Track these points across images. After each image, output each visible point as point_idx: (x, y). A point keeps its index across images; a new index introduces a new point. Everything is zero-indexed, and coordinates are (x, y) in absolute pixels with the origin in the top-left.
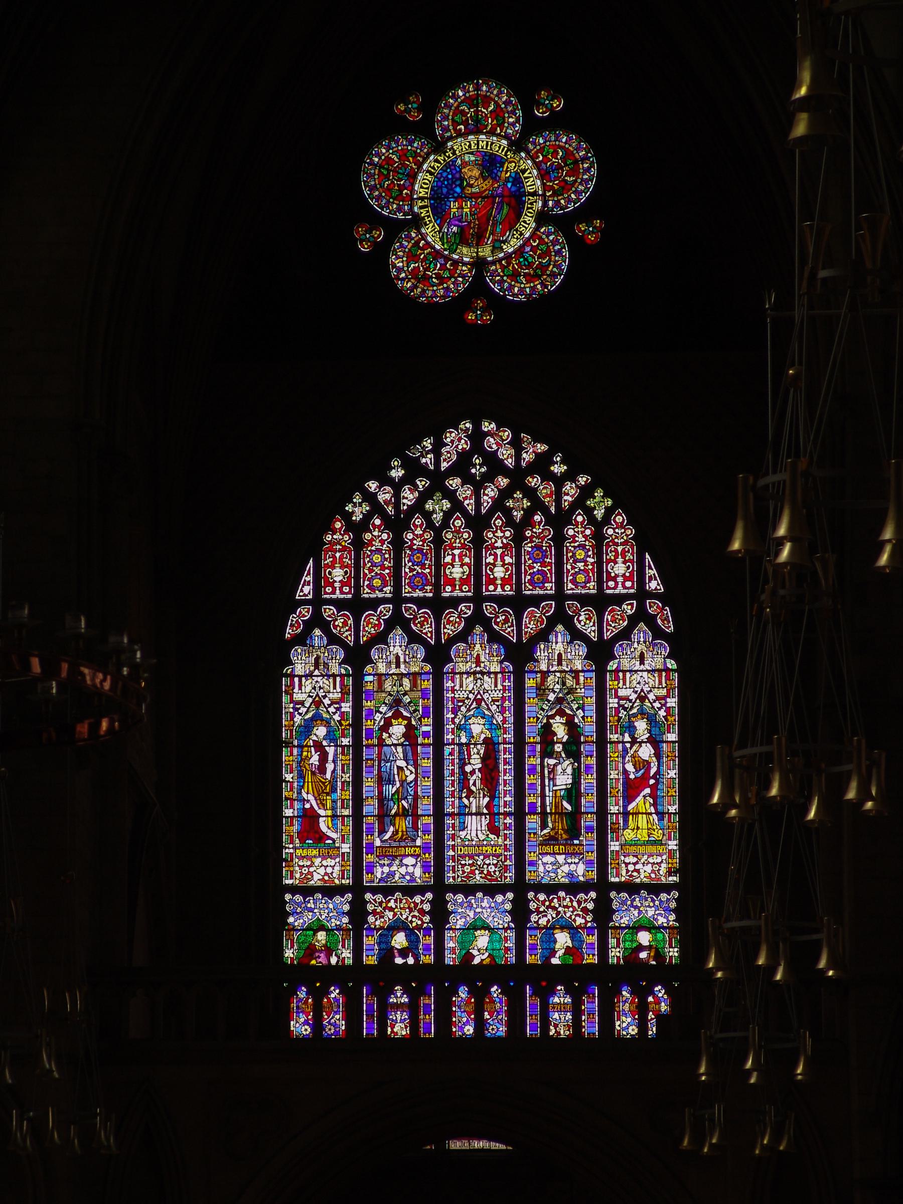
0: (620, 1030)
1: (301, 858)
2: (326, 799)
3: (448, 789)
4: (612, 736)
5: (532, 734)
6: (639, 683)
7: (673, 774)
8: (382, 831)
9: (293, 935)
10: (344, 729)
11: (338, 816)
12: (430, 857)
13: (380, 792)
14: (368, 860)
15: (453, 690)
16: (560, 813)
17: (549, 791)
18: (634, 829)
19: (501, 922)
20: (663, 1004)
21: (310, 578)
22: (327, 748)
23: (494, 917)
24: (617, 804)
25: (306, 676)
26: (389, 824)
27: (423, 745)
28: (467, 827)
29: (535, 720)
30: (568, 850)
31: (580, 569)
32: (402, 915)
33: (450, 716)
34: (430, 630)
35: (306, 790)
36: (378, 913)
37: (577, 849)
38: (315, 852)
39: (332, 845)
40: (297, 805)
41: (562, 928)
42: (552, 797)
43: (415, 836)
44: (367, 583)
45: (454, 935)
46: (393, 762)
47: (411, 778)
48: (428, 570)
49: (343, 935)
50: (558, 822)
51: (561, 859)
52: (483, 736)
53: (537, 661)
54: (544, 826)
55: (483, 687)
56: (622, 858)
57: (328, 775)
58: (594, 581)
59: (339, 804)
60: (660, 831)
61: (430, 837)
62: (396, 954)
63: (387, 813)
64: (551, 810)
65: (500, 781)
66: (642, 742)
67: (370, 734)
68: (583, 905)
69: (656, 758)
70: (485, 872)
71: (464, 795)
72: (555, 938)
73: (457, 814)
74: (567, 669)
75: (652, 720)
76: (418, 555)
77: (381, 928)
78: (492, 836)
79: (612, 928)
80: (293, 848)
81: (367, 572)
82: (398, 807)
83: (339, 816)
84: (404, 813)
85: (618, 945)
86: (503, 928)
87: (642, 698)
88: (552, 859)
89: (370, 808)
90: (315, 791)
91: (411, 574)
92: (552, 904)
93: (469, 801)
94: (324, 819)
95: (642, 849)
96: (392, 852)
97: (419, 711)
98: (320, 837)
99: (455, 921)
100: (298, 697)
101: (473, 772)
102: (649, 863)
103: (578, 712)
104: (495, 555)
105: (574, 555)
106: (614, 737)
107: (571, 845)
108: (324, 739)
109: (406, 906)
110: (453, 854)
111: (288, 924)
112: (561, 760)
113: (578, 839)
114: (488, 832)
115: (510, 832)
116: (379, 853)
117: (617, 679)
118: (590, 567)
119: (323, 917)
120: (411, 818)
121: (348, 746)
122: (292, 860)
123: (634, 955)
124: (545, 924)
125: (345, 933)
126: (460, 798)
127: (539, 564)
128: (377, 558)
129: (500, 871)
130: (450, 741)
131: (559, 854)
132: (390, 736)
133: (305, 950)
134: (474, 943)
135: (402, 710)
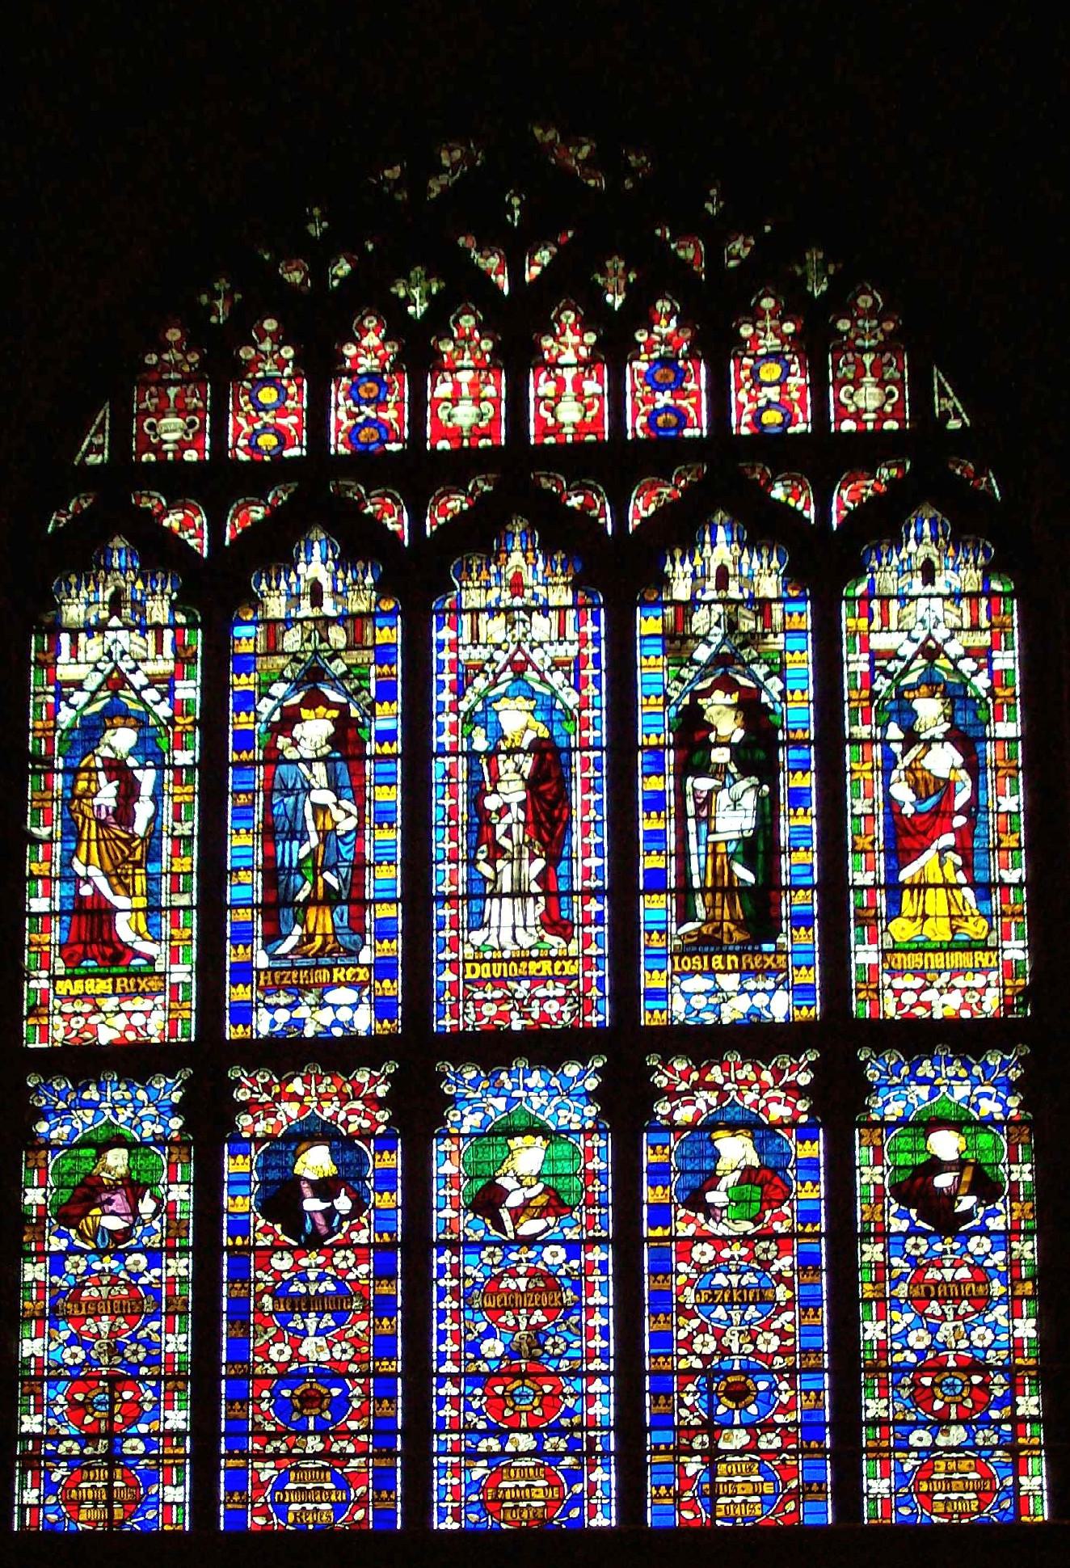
1: (70, 998)
2: (134, 875)
3: (442, 843)
4: (855, 729)
6: (922, 621)
7: (1011, 803)
8: (273, 936)
9: (46, 1159)
10: (182, 733)
11: (160, 909)
12: (392, 988)
13: (270, 859)
14: (235, 998)
16: (728, 889)
17: (698, 844)
19: (576, 1118)
20: (996, 1283)
21: (103, 440)
22: (138, 774)
25: (90, 630)
26: (291, 920)
27: (377, 758)
29: (661, 700)
30: (748, 965)
31: (769, 402)
33: (447, 697)
35: (83, 856)
38: (104, 986)
39: (148, 969)
41: (733, 1127)
42: (707, 854)
43: (355, 943)
44: (242, 442)
49: (170, 1154)
50: (722, 907)
51: (730, 982)
52: (530, 736)
54: (685, 914)
56: (887, 979)
57: (140, 827)
59: (166, 882)
60: (984, 922)
62: (307, 1192)
63: (285, 897)
64: (703, 881)
66: (933, 740)
70: (536, 1015)
72: (718, 1151)
74: (739, 596)
75: (956, 695)
76: (369, 385)
77: (268, 1137)
80: (48, 978)
81: (242, 421)
82: (315, 885)
83: (166, 909)
84: (330, 899)
85: (878, 1160)
86: (582, 1130)
87: (931, 653)
88: (708, 984)
89: (245, 887)
91: (351, 423)
92: (708, 1078)
93: (495, 869)
95: (937, 960)
96: (298, 978)
97: (369, 691)
98: (116, 955)
99: (458, 1118)
100: (65, 672)
101: (505, 809)
102: (954, 987)
103: (769, 683)
104: (561, 382)
105: (755, 373)
106: (862, 731)
107: (754, 953)
109: (334, 1089)
110: (454, 978)
113: (773, 941)
114: (543, 932)
115: (600, 929)
119: (122, 1119)
120: (345, 908)
121: (190, 768)
122: (45, 1004)
125: (175, 1150)
126: (472, 862)
127: (668, 393)
128: (268, 395)
129: (573, 1013)
130: (447, 748)
131: (725, 972)
132: (295, 743)
133: (74, 1188)
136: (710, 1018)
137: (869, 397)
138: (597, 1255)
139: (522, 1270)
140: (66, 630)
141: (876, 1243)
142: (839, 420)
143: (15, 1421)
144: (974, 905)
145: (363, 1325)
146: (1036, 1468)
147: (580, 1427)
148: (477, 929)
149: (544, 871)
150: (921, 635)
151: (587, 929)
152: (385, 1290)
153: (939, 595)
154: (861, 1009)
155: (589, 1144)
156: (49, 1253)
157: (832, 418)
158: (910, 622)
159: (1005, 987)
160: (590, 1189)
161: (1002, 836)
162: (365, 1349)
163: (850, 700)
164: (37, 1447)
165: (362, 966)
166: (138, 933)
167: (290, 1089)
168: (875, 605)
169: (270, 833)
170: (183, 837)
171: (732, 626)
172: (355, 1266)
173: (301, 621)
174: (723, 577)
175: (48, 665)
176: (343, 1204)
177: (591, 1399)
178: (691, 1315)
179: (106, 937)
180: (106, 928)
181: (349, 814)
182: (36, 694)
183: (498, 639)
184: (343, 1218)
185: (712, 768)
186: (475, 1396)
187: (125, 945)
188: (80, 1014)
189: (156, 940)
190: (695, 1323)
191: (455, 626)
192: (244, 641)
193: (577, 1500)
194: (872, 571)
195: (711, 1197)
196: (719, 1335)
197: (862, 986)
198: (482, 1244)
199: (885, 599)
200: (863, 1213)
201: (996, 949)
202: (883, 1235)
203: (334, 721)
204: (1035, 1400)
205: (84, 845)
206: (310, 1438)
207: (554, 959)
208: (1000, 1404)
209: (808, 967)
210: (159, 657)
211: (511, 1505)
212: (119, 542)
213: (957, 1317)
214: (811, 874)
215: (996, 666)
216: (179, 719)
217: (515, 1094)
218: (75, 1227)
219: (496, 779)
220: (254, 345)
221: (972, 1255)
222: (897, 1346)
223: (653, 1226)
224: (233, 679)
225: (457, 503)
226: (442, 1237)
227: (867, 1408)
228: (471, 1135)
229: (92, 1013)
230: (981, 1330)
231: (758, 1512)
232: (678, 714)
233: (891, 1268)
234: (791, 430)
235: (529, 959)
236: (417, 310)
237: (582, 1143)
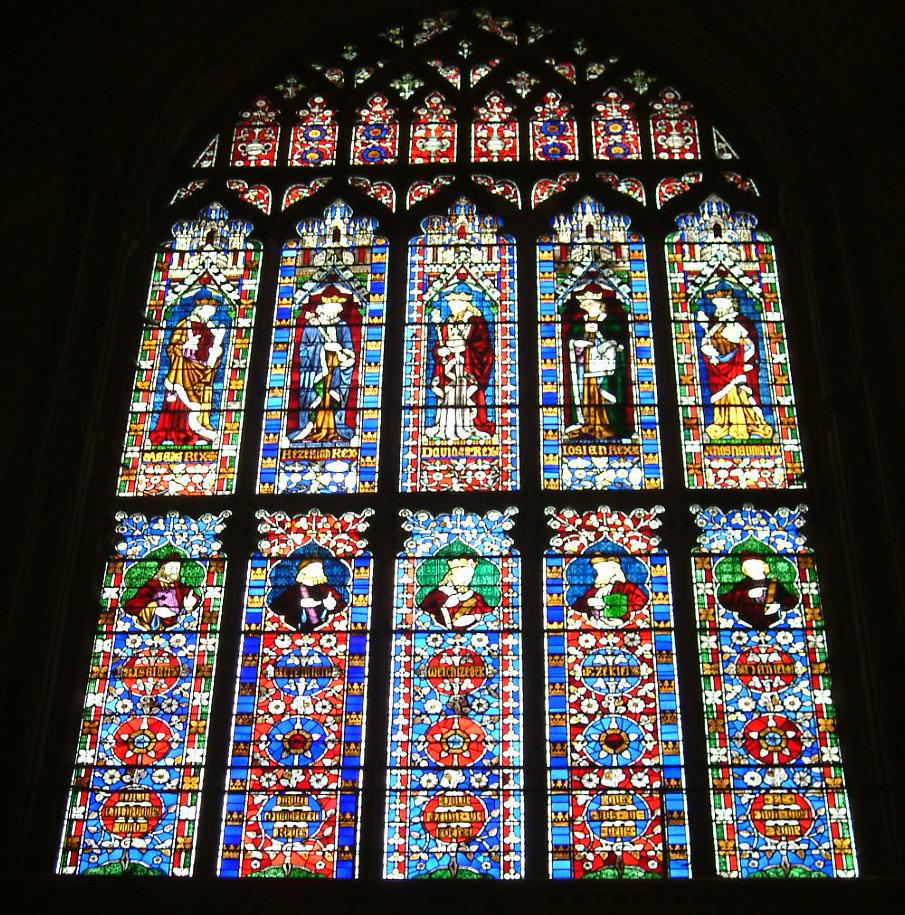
0: (722, 705)
2: (204, 390)
3: (408, 375)
4: (677, 315)
5: (547, 308)
8: (293, 428)
9: (122, 568)
11: (220, 411)
13: (295, 383)
15: (421, 264)
17: (578, 378)
18: (723, 425)
19: (496, 548)
20: (799, 665)
21: (214, 154)
22: (213, 331)
23: (483, 541)
24: (692, 393)
25: (192, 252)
26: (306, 419)
29: (553, 296)
30: (613, 452)
31: (615, 143)
33: (416, 292)
34: (389, 201)
35: (172, 379)
38: (177, 457)
41: (606, 556)
43: (349, 434)
44: (296, 157)
47: (347, 363)
48: (390, 144)
49: (210, 566)
50: (595, 416)
51: (601, 462)
52: (468, 315)
53: (555, 233)
54: (570, 420)
55: (469, 260)
56: (707, 462)
57: (211, 362)
59: (225, 395)
60: (769, 428)
62: (305, 593)
65: (496, 366)
66: (727, 321)
69: (751, 339)
70: (469, 481)
71: (435, 383)
72: (595, 570)
73: (422, 408)
74: (601, 241)
75: (740, 297)
78: (483, 434)
81: (297, 146)
83: (224, 411)
84: (334, 407)
85: (709, 579)
86: (501, 556)
89: (276, 400)
90: (188, 382)
91: (364, 148)
92: (588, 523)
95: (740, 451)
96: (309, 455)
97: (366, 287)
98: (185, 437)
99: (414, 546)
100: (174, 273)
102: (752, 468)
103: (621, 288)
105: (606, 129)
106: (682, 316)
107: (617, 445)
108: (210, 320)
109: (328, 526)
110: (414, 456)
111: (117, 553)
112: (597, 342)
114: (475, 429)
115: (513, 428)
116: (287, 456)
117: (683, 252)
118: (631, 140)
120: (344, 412)
122: (135, 467)
123: (738, 593)
126: (429, 387)
128: (314, 134)
131: (598, 456)
132: (317, 316)
133: (140, 588)
135: (339, 287)
136: (588, 485)
137: (675, 141)
139: (456, 650)
140: (178, 251)
142: (657, 153)
143: (74, 753)
144: (762, 418)
145: (339, 688)
146: (841, 801)
147: (497, 766)
148: (431, 427)
150: (717, 264)
151: (505, 428)
152: (357, 663)
153: (725, 243)
154: (691, 482)
155: (505, 565)
156: (116, 633)
157: (654, 151)
158: (708, 257)
159: (787, 469)
160: (506, 595)
162: (339, 706)
163: (673, 298)
164: (88, 774)
165: (352, 448)
166: (203, 425)
167: (298, 525)
169: (296, 367)
170: (239, 368)
171: (597, 257)
173: (325, 249)
174: (590, 230)
175: (164, 269)
176: (330, 602)
177: (506, 744)
178: (579, 684)
179: (182, 427)
180: (182, 421)
181: (349, 357)
184: (329, 612)
185: (586, 335)
186: (419, 742)
190: (582, 691)
191: (422, 253)
192: (289, 259)
193: (495, 821)
194: (683, 229)
195: (591, 602)
196: (600, 699)
197: (691, 466)
198: (429, 632)
200: (700, 615)
202: (715, 630)
203: (343, 304)
206: (294, 771)
207: (482, 447)
208: (811, 752)
209: (654, 454)
210: (234, 267)
211: (444, 825)
212: (217, 206)
215: (764, 281)
217: (454, 531)
218: (137, 615)
219: (446, 339)
220: (308, 109)
222: (731, 709)
223: (551, 622)
226: (399, 626)
227: (711, 755)
228: (423, 558)
230: (791, 699)
231: (634, 834)
232: (563, 304)
233: (723, 653)
234: (629, 157)
235: (465, 446)
236: (407, 95)
237: (500, 564)
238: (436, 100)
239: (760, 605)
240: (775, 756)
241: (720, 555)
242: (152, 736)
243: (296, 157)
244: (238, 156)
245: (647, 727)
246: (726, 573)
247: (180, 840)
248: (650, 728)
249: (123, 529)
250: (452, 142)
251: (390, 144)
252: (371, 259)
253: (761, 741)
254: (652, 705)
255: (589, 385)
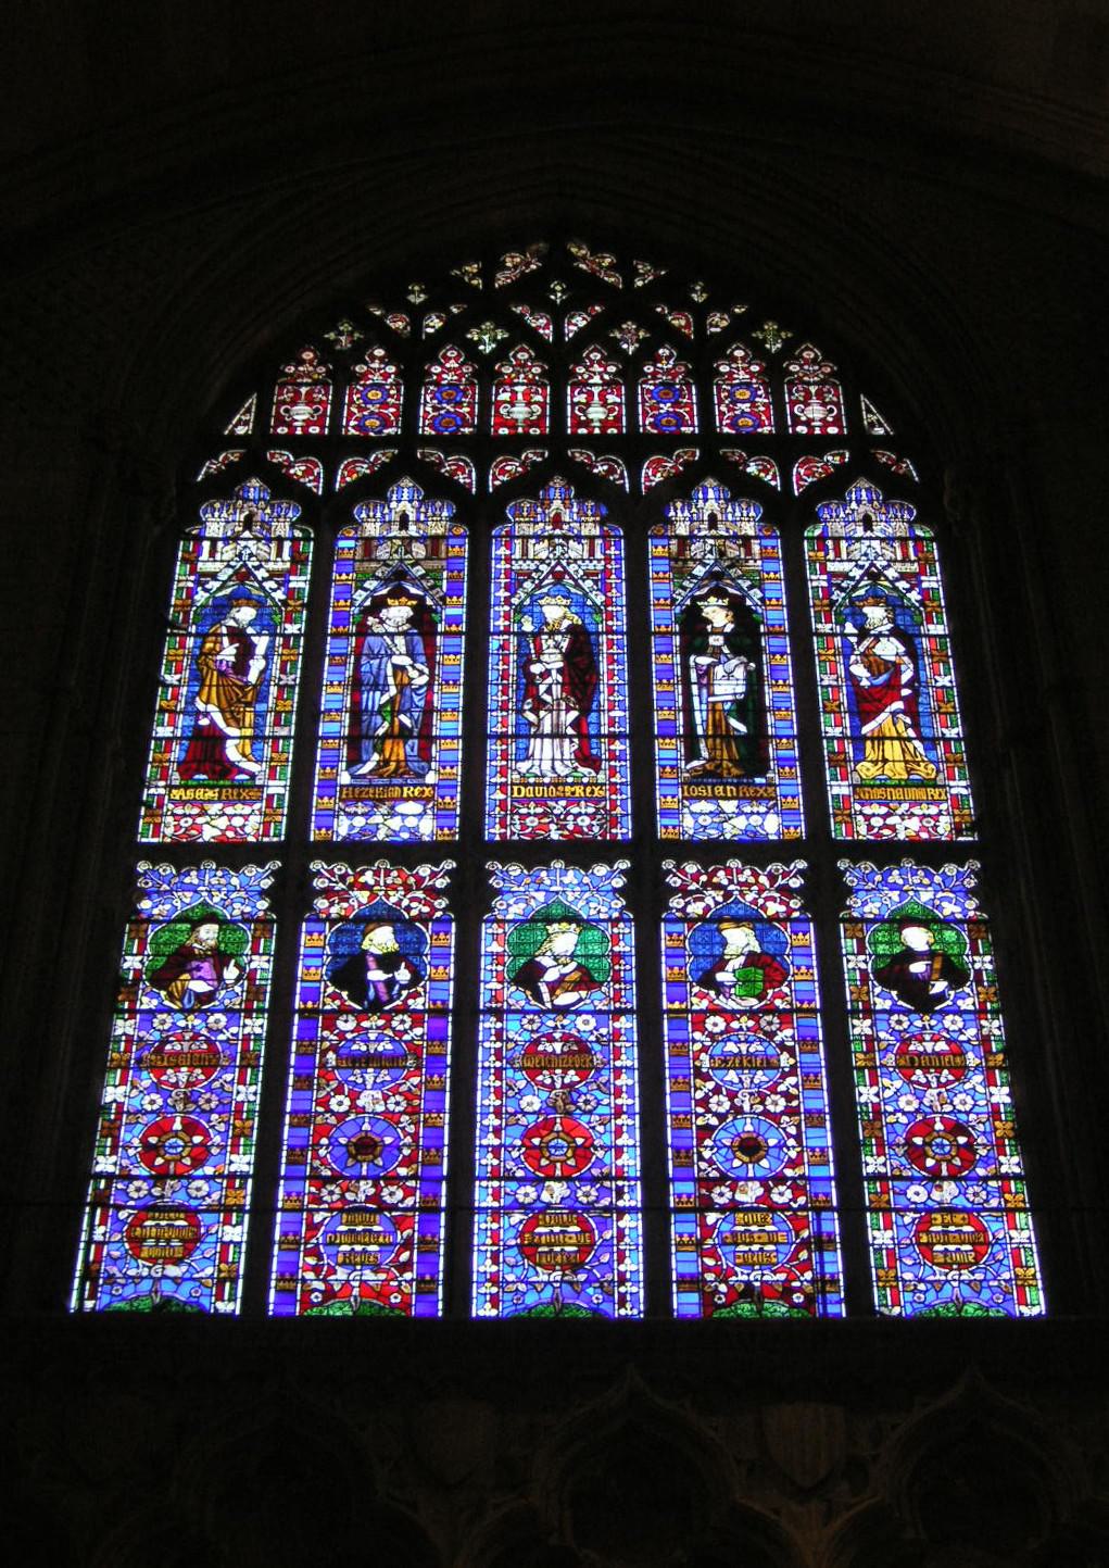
1: (183, 803)
3: (494, 696)
4: (819, 626)
5: (661, 618)
6: (866, 555)
8: (355, 760)
9: (146, 931)
11: (264, 738)
13: (356, 702)
15: (508, 559)
16: (720, 733)
17: (701, 703)
19: (604, 909)
20: (970, 1055)
21: (251, 417)
22: (255, 639)
25: (226, 540)
26: (371, 749)
28: (533, 755)
29: (668, 602)
32: (388, 897)
33: (503, 594)
34: (468, 481)
35: (204, 698)
36: (337, 893)
37: (761, 791)
38: (210, 794)
40: (181, 721)
41: (738, 921)
42: (708, 711)
43: (423, 768)
44: (352, 423)
45: (500, 931)
46: (385, 659)
48: (468, 409)
49: (255, 930)
51: (730, 806)
52: (566, 623)
53: (670, 522)
54: (692, 753)
56: (858, 807)
57: (253, 677)
58: (770, 425)
60: (931, 766)
61: (454, 771)
64: (705, 730)
67: (341, 619)
68: (780, 882)
69: (910, 657)
72: (724, 939)
75: (895, 604)
77: (342, 918)
78: (586, 770)
79: (844, 921)
80: (165, 787)
81: (354, 410)
83: (269, 737)
84: (404, 734)
85: (861, 951)
86: (609, 919)
89: (333, 727)
90: (223, 698)
92: (715, 880)
93: (538, 715)
94: (237, 741)
95: (897, 794)
97: (441, 587)
98: (225, 769)
100: (205, 566)
101: (546, 674)
102: (912, 815)
103: (751, 592)
105: (731, 395)
106: (826, 628)
107: (749, 785)
109: (399, 881)
110: (502, 797)
112: (723, 658)
113: (763, 775)
117: (825, 549)
118: (762, 409)
120: (416, 741)
121: (297, 637)
122: (161, 805)
123: (897, 967)
124: (701, 912)
125: (260, 926)
126: (519, 711)
129: (601, 826)
131: (726, 798)
132: (382, 622)
133: (169, 956)
134: (546, 945)
136: (714, 833)
137: (815, 412)
138: (626, 1023)
139: (557, 1035)
140: (208, 539)
141: (864, 1019)
143: (90, 1160)
144: (922, 752)
145: (415, 1080)
146: (1023, 1222)
147: (608, 1177)
148: (523, 760)
149: (577, 719)
150: (867, 564)
151: (613, 763)
152: (437, 1050)
153: (877, 538)
154: (838, 832)
155: (616, 930)
156: (141, 1011)
158: (856, 555)
159: (954, 816)
160: (617, 967)
161: (942, 704)
162: (416, 1102)
163: (814, 606)
164: (109, 1186)
165: (428, 786)
166: (244, 755)
167: (362, 879)
168: (830, 543)
169: (357, 685)
170: (286, 685)
171: (722, 554)
172: (411, 1028)
173: (391, 539)
174: (713, 521)
175: (191, 561)
176: (403, 975)
177: (619, 1151)
178: (707, 1078)
179: (217, 757)
181: (421, 673)
182: (179, 581)
183: (543, 555)
184: (403, 987)
185: (710, 650)
186: (514, 1147)
187: (232, 764)
188: (190, 816)
189: (259, 761)
190: (710, 1085)
191: (509, 546)
192: (346, 551)
193: (607, 1244)
194: (826, 521)
195: (720, 977)
198: (524, 1012)
199: (836, 540)
200: (852, 993)
201: (944, 786)
202: (869, 1012)
203: (413, 607)
204: (1016, 1159)
205: (207, 689)
206: (362, 1183)
207: (586, 785)
208: (986, 1161)
209: (794, 797)
211: (546, 1249)
212: (255, 482)
213: (940, 1085)
214: (792, 728)
215: (925, 585)
216: (291, 602)
217: (553, 889)
219: (539, 652)
220: (366, 363)
221: (948, 1031)
224: (335, 576)
225: (514, 467)
226: (488, 1005)
227: (867, 1164)
228: (514, 921)
229: (199, 815)
232: (682, 612)
234: (760, 430)
235: (566, 784)
236: (488, 348)
237: (610, 930)
238: (522, 356)
239: (924, 982)
240: (944, 1166)
241: (874, 921)
242: (187, 1139)
243: (352, 423)
244: (281, 421)
245: (788, 1130)
246: (881, 943)
247: (223, 1266)
248: (793, 1130)
249: (147, 883)
250: (544, 408)
251: (468, 409)
252: (447, 552)
253: (927, 1148)
254: (795, 1103)
255: (714, 710)
